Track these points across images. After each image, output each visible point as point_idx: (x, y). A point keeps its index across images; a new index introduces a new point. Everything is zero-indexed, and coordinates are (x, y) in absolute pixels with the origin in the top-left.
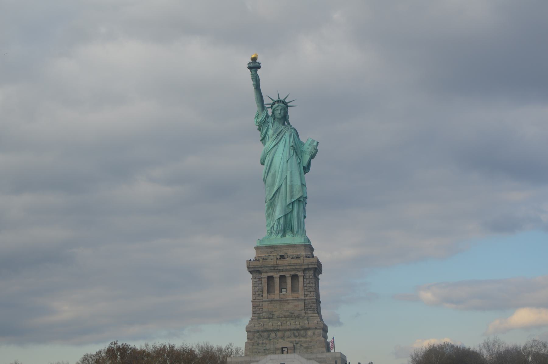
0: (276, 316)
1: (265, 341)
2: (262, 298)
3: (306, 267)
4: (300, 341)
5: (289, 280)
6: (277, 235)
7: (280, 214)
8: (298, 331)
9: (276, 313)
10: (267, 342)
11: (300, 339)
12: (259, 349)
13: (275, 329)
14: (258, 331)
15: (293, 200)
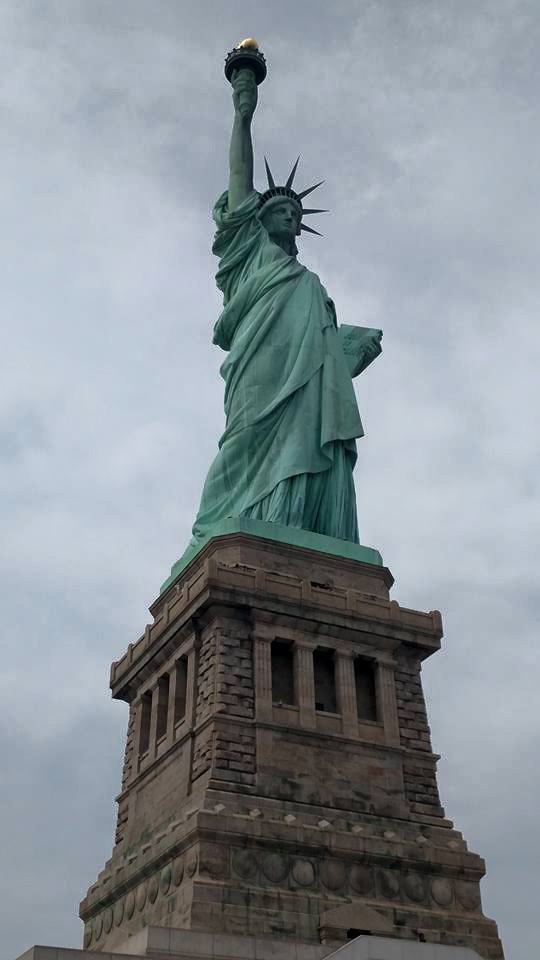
0: (304, 796)
1: (273, 890)
2: (249, 712)
3: (408, 638)
4: (412, 916)
5: (345, 672)
6: (285, 523)
7: (295, 465)
8: (397, 872)
9: (303, 781)
10: (283, 897)
11: (406, 908)
12: (251, 921)
13: (315, 846)
14: (246, 841)
15: (342, 438)
